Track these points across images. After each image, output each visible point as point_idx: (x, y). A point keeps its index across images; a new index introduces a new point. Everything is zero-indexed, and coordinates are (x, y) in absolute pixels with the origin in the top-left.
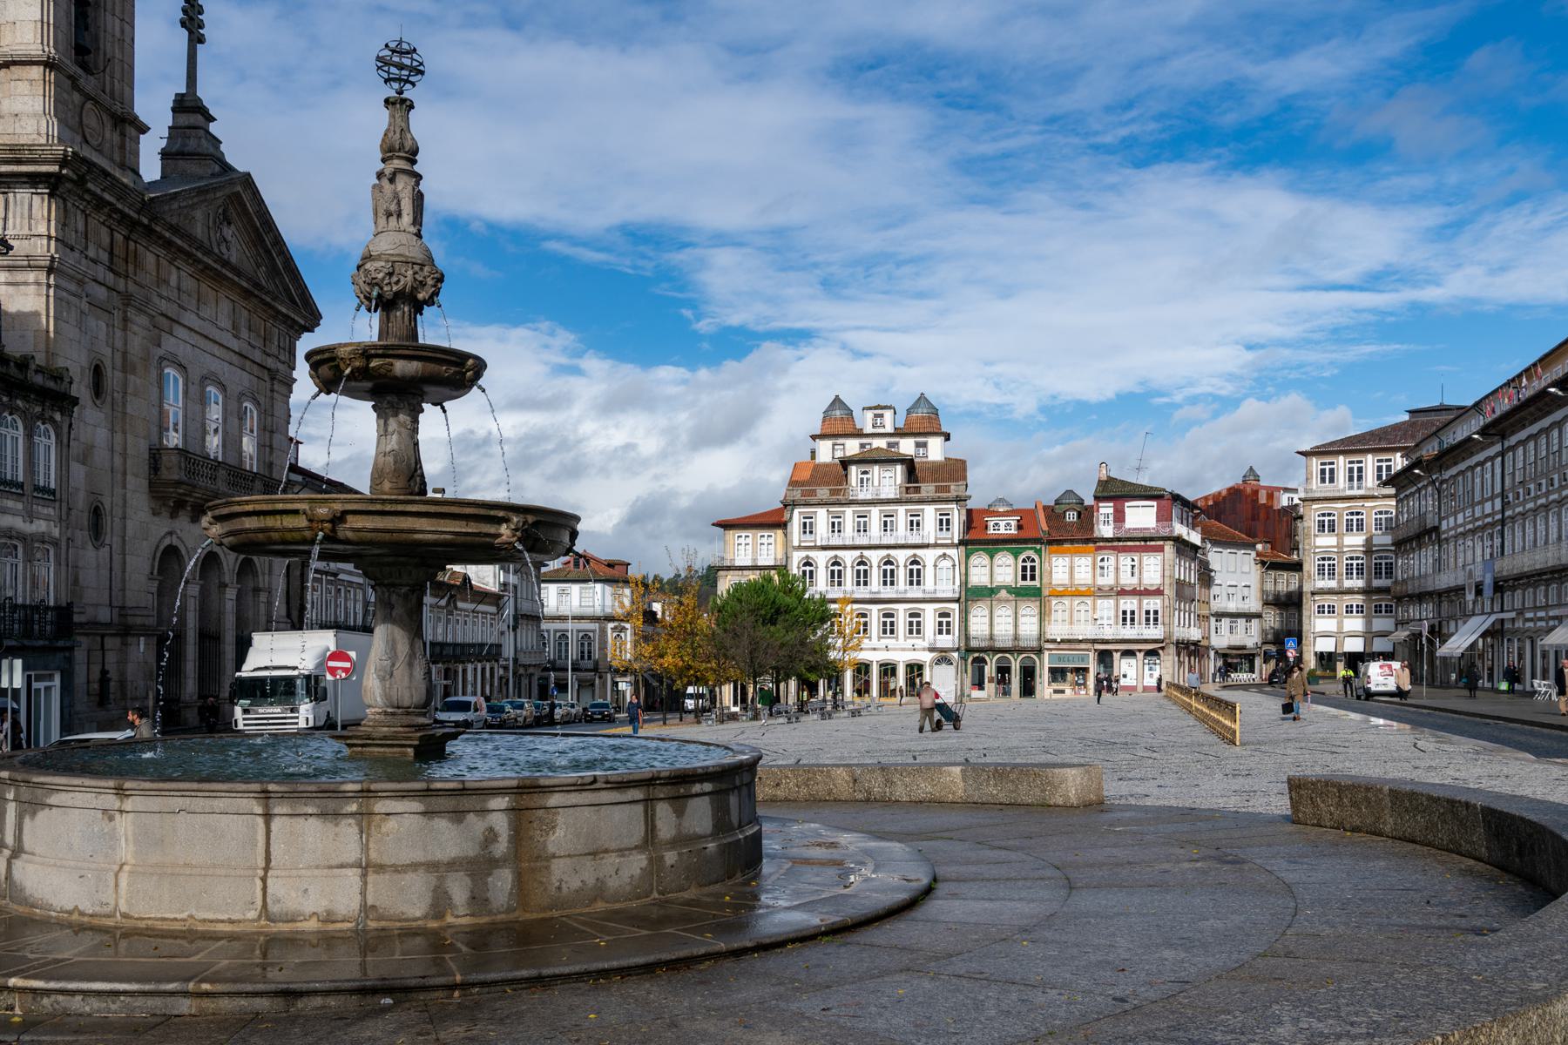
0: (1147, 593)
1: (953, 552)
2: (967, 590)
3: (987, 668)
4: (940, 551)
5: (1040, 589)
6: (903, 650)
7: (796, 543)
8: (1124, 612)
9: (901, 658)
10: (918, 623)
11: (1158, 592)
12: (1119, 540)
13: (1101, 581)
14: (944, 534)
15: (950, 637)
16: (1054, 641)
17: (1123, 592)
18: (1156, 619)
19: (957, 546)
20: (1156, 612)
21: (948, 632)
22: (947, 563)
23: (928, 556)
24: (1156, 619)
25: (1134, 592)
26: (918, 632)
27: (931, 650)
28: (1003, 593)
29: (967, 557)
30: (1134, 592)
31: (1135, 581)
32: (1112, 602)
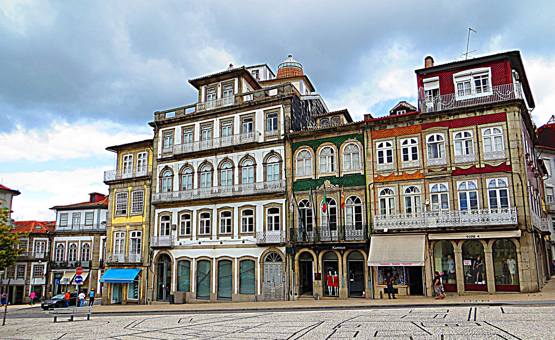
0: (489, 170)
1: (279, 149)
2: (294, 184)
3: (314, 264)
4: (268, 150)
5: (364, 176)
6: (238, 246)
7: (159, 157)
8: (463, 196)
9: (236, 254)
10: (251, 220)
11: (505, 169)
12: (449, 113)
13: (430, 162)
14: (273, 132)
15: (278, 232)
16: (381, 232)
17: (459, 173)
18: (504, 202)
19: (284, 142)
20: (503, 193)
21: (277, 228)
22: (275, 160)
23: (259, 154)
24: (504, 202)
25: (473, 171)
26: (251, 229)
27: (260, 245)
28: (327, 183)
29: (293, 152)
30: (473, 171)
31: (472, 158)
32: (446, 184)
